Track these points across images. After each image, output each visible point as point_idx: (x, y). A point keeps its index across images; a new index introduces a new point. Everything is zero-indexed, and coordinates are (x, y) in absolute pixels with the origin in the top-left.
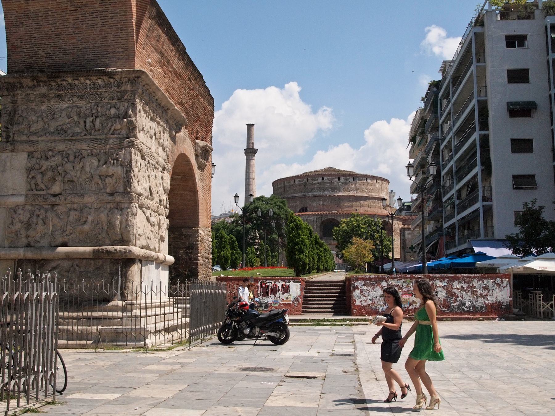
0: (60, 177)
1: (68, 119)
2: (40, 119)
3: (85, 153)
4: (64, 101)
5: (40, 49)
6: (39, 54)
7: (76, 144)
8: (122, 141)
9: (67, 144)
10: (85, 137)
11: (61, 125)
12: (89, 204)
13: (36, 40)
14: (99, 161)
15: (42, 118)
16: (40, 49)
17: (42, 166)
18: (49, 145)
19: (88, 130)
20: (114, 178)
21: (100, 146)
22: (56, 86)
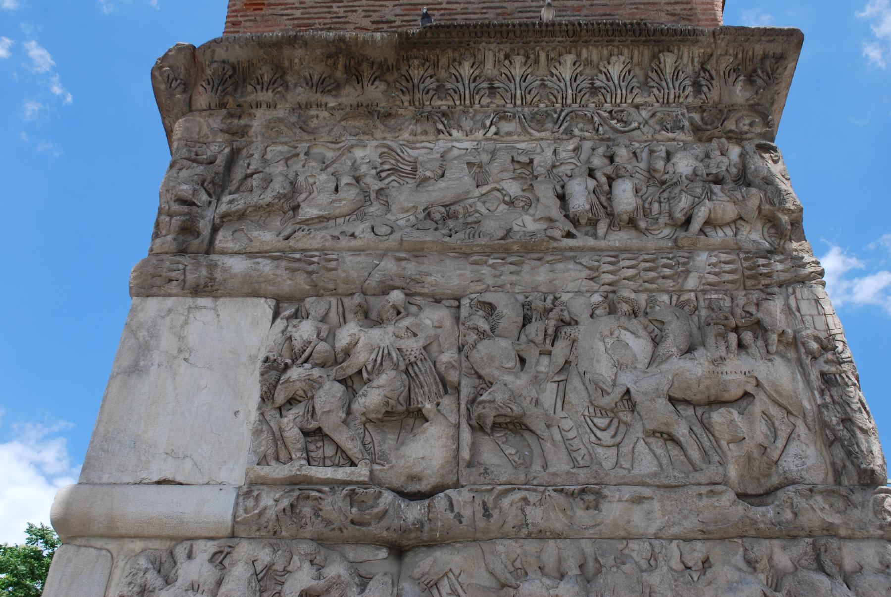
0: (447, 402)
1: (478, 186)
2: (345, 180)
3: (578, 307)
4: (460, 128)
6: (348, 22)
7: (526, 268)
8: (762, 261)
9: (485, 270)
10: (571, 242)
11: (445, 206)
12: (633, 545)
14: (656, 342)
15: (358, 180)
16: (356, 11)
17: (347, 353)
18: (389, 266)
19: (583, 221)
20: (757, 407)
21: (652, 275)
22: (428, 81)
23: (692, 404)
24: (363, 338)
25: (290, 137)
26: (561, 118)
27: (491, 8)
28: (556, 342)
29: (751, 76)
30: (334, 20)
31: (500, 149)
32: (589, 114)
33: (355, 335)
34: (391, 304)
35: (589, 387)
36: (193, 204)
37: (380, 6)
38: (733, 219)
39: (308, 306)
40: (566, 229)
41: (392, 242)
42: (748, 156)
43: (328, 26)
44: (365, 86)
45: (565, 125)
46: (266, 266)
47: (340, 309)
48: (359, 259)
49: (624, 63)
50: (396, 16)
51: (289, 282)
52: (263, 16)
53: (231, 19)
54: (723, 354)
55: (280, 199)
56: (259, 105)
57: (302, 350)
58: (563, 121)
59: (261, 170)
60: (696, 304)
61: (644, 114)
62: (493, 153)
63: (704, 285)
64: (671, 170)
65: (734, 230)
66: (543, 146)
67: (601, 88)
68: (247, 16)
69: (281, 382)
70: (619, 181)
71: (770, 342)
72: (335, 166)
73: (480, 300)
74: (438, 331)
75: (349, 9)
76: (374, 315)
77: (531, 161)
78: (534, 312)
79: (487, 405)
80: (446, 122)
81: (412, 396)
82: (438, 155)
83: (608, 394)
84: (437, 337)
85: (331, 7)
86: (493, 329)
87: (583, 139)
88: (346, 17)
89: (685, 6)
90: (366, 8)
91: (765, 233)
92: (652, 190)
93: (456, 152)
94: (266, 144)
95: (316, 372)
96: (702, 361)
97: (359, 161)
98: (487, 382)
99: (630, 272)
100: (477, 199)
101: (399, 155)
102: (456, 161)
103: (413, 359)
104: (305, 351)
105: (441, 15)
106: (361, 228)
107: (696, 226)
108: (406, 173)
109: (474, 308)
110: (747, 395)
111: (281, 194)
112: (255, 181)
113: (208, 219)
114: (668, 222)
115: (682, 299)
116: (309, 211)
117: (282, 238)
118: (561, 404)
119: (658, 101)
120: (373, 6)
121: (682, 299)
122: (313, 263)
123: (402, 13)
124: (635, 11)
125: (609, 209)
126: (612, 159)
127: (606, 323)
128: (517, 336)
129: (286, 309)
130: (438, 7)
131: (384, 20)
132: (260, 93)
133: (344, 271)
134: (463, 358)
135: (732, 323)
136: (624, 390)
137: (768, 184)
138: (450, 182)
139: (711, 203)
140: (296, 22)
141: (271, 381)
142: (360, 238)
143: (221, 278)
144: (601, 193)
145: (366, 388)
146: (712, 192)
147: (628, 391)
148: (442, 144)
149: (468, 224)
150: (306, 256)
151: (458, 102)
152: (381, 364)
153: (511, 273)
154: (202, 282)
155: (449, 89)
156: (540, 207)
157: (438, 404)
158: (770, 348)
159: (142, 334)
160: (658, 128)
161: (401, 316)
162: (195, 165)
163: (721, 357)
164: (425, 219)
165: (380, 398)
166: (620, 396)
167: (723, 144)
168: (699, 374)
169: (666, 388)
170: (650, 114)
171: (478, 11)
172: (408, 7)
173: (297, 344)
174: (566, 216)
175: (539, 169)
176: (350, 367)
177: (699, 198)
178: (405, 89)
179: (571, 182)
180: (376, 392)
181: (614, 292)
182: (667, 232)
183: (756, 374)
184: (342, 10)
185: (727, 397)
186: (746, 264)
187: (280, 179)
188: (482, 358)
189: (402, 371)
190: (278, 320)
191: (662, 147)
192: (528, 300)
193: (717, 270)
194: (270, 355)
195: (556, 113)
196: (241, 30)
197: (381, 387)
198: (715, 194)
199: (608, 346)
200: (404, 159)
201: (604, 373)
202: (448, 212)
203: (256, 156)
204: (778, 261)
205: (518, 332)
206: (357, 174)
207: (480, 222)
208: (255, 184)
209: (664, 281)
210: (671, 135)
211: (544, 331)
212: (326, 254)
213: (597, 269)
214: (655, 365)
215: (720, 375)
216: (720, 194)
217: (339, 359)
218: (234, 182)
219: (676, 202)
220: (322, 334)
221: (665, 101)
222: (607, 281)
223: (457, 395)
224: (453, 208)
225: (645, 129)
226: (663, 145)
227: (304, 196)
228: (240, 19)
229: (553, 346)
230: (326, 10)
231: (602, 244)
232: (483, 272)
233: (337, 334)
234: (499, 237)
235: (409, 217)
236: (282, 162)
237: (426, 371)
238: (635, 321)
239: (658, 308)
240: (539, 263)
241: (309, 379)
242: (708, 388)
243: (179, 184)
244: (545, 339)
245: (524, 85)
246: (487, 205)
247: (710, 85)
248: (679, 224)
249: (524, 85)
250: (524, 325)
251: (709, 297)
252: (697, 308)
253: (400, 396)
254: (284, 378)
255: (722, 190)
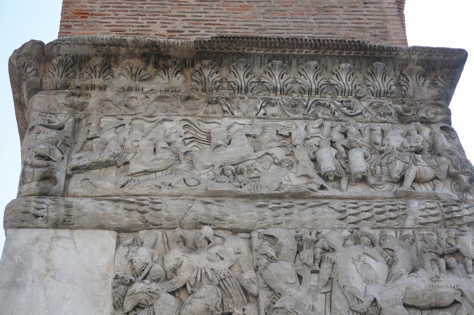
1: (255, 151)
5: (155, 23)
7: (295, 210)
8: (455, 208)
9: (267, 212)
13: (146, 6)
14: (390, 264)
16: (155, 23)
17: (174, 271)
19: (331, 178)
21: (382, 216)
23: (419, 309)
24: (185, 261)
25: (117, 112)
26: (309, 105)
27: (251, 25)
28: (322, 265)
29: (434, 80)
30: (140, 28)
31: (267, 126)
32: (327, 103)
33: (179, 258)
34: (204, 236)
35: (348, 297)
36: (49, 159)
37: (172, 20)
38: (432, 178)
39: (141, 237)
40: (321, 184)
41: (200, 189)
42: (436, 135)
43: (136, 32)
44: (170, 77)
45: (312, 110)
46: (109, 207)
47: (165, 240)
48: (176, 202)
49: (349, 68)
50: (184, 27)
51: (127, 219)
52: (87, 22)
53: (64, 23)
54: (437, 274)
55: (115, 157)
56: (93, 87)
57: (141, 270)
58: (310, 107)
59: (98, 135)
60: (413, 238)
61: (365, 104)
62: (264, 129)
63: (417, 224)
64: (385, 142)
65: (432, 186)
66: (298, 124)
67: (334, 85)
68: (77, 22)
69: (128, 294)
70: (353, 150)
71: (468, 265)
72: (151, 134)
73: (266, 233)
74: (238, 256)
75: (151, 21)
76: (190, 244)
77: (290, 134)
78: (305, 243)
79: (280, 310)
80: (229, 105)
81: (225, 304)
82: (225, 129)
83: (362, 302)
84: (237, 261)
85: (137, 19)
86: (277, 254)
87: (325, 119)
88: (149, 26)
89: (382, 30)
90: (162, 21)
91: (453, 189)
92: (374, 157)
93: (236, 127)
94: (100, 117)
95: (154, 286)
96: (424, 278)
97: (168, 131)
98: (277, 294)
99: (368, 215)
100: (254, 161)
101: (197, 127)
102: (238, 133)
103: (223, 277)
104: (144, 270)
105: (216, 28)
106: (175, 180)
107: (408, 182)
108: (203, 141)
109: (261, 240)
110: (455, 302)
111: (116, 154)
112: (95, 144)
113: (62, 171)
114: (388, 180)
115: (403, 234)
116: (135, 167)
117: (118, 187)
118: (329, 309)
119: (373, 96)
120: (168, 19)
121: (403, 234)
122: (143, 205)
123: (189, 26)
124: (349, 32)
125: (347, 170)
126: (345, 134)
127: (355, 251)
128: (294, 260)
129: (125, 239)
130: (214, 23)
131: (176, 30)
132: (94, 79)
133: (167, 212)
134: (259, 276)
135: (440, 251)
136: (373, 299)
137: (452, 155)
138: (235, 148)
139: (417, 167)
140: (112, 28)
141: (121, 293)
142: (177, 187)
143: (75, 215)
144: (341, 159)
145: (190, 298)
146: (416, 160)
147: (375, 300)
148: (227, 121)
149: (251, 178)
150: (137, 200)
151: (236, 92)
152: (201, 280)
153: (285, 214)
154: (61, 218)
155: (230, 82)
156: (300, 167)
157: (244, 310)
158: (468, 269)
159: (17, 257)
160: (374, 113)
161: (211, 245)
162: (48, 130)
163: (436, 276)
164: (221, 174)
165: (202, 305)
166: (370, 303)
167: (418, 126)
168: (423, 288)
169: (402, 297)
170: (368, 104)
171: (241, 27)
172: (193, 22)
173: (138, 266)
174: (319, 174)
175: (296, 140)
176: (178, 282)
177: (408, 163)
178: (199, 81)
179: (320, 151)
180: (200, 301)
181: (357, 229)
182: (388, 186)
183: (461, 288)
184: (146, 21)
185: (443, 304)
186: (444, 210)
187: (113, 142)
188: (272, 276)
189: (216, 285)
190: (121, 247)
191: (378, 127)
192: (299, 234)
193: (426, 214)
194: (119, 273)
195: (305, 101)
196: (72, 31)
197: (203, 297)
198: (418, 161)
199: (358, 267)
200: (201, 130)
201: (358, 287)
202: (236, 169)
203: (93, 125)
204: (465, 208)
205: (294, 257)
206: (169, 140)
207: (259, 177)
208: (94, 146)
209: (391, 221)
210: (383, 119)
211: (313, 257)
212: (153, 199)
213: (344, 211)
214: (391, 281)
215: (437, 288)
216: (422, 161)
217: (169, 277)
218: (79, 143)
219: (393, 166)
220: (154, 258)
221: (378, 96)
222: (352, 221)
223: (256, 303)
224: (239, 166)
225: (366, 114)
226: (379, 126)
227: (131, 155)
228: (71, 24)
229: (320, 267)
230: (134, 21)
231: (346, 194)
232: (266, 213)
233: (166, 258)
234: (275, 189)
235: (209, 173)
236: (112, 130)
237: (233, 285)
238: (374, 249)
239: (388, 240)
240: (304, 207)
241: (149, 292)
242: (430, 298)
243: (38, 144)
244: (314, 262)
245: (282, 81)
246: (262, 165)
247: (407, 86)
248: (396, 181)
249: (282, 81)
250: (298, 252)
251: (422, 233)
252: (414, 241)
253: (216, 304)
254: (130, 291)
255: (423, 158)
